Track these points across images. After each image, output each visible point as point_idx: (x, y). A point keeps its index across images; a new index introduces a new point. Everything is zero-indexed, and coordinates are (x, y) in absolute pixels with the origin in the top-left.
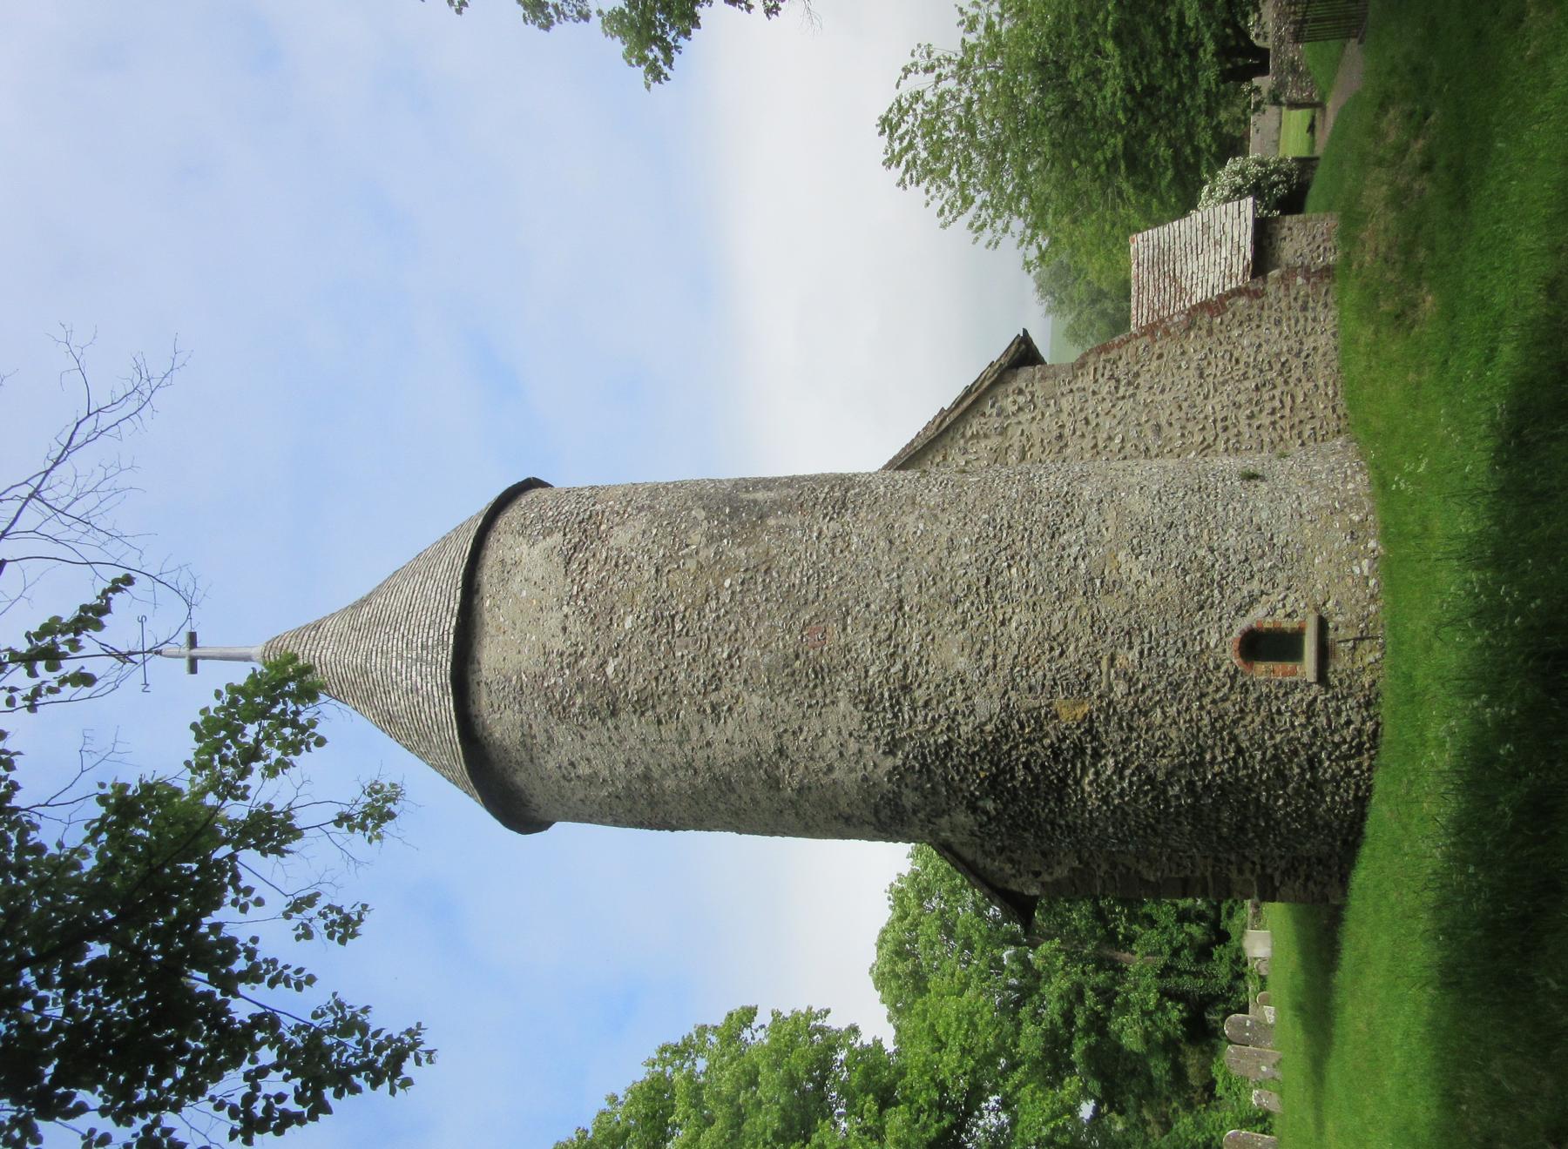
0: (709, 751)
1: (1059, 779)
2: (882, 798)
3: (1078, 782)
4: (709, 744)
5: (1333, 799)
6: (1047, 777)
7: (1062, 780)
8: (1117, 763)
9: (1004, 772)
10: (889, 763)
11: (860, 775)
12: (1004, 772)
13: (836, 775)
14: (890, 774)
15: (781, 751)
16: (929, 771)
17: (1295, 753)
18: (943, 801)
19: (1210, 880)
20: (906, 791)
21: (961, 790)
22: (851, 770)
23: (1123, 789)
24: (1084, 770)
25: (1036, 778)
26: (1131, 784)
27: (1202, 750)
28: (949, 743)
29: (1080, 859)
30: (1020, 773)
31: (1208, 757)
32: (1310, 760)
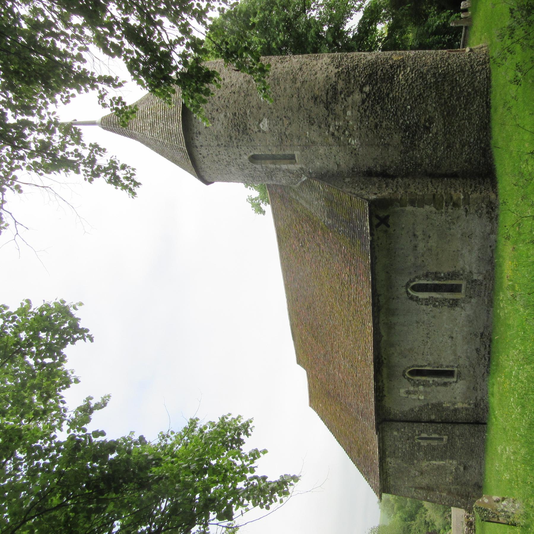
0: (276, 70)
1: (392, 75)
2: (331, 85)
3: (398, 76)
4: (276, 68)
5: (480, 78)
6: (388, 74)
7: (393, 75)
8: (411, 69)
9: (374, 73)
10: (336, 70)
11: (326, 75)
12: (374, 73)
13: (318, 75)
14: (336, 74)
15: (301, 69)
16: (349, 73)
17: (466, 64)
18: (351, 86)
19: (444, 194)
20: (340, 81)
21: (359, 81)
22: (323, 73)
23: (412, 77)
24: (400, 72)
25: (384, 75)
26: (415, 74)
27: (438, 65)
28: (357, 65)
29: (393, 190)
30: (379, 72)
31: (439, 66)
32: (471, 66)
